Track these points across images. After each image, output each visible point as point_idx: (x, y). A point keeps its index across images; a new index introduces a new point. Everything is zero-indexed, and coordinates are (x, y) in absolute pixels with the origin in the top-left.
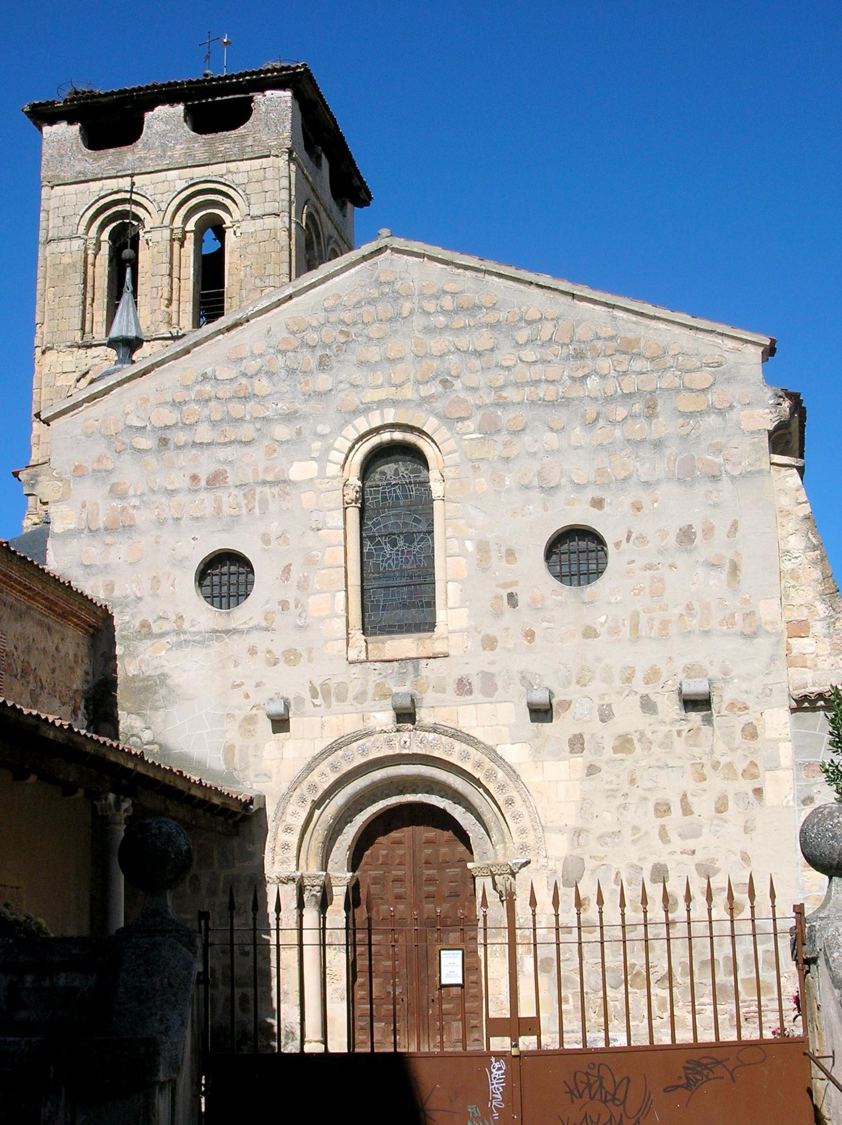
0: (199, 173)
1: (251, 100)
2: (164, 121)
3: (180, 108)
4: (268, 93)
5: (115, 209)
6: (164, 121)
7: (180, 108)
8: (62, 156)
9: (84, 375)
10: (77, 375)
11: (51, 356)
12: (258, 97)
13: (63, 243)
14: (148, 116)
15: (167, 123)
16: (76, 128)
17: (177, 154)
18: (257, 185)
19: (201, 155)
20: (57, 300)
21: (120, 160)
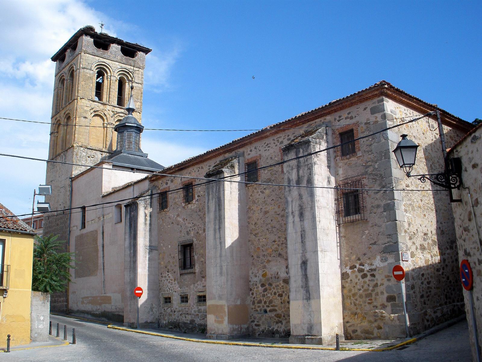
0: (124, 66)
1: (136, 52)
2: (115, 48)
3: (120, 47)
4: (141, 52)
5: (102, 66)
6: (115, 48)
7: (120, 47)
8: (88, 46)
9: (92, 109)
10: (90, 108)
11: (83, 100)
12: (139, 52)
13: (88, 70)
14: (112, 45)
15: (116, 49)
16: (93, 40)
17: (119, 58)
18: (137, 75)
19: (124, 61)
20: (86, 85)
21: (104, 54)
